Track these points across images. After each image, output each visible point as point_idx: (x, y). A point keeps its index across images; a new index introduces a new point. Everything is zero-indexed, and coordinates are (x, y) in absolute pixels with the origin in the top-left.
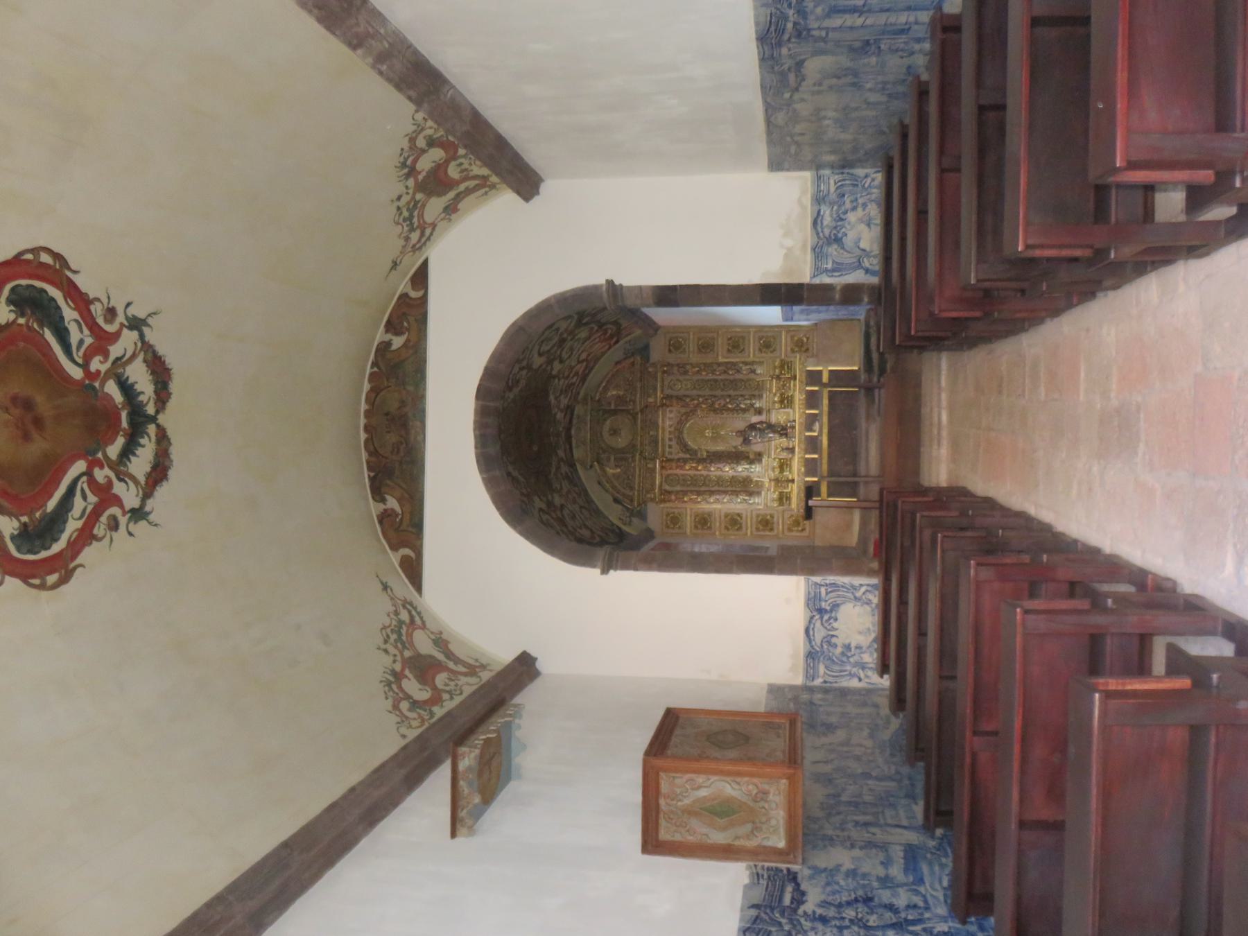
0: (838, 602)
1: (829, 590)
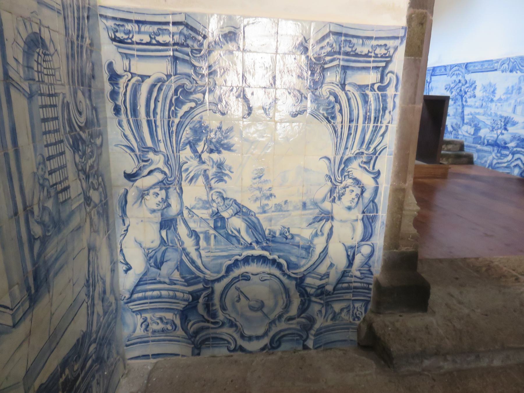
0: (339, 118)
1: (368, 92)
